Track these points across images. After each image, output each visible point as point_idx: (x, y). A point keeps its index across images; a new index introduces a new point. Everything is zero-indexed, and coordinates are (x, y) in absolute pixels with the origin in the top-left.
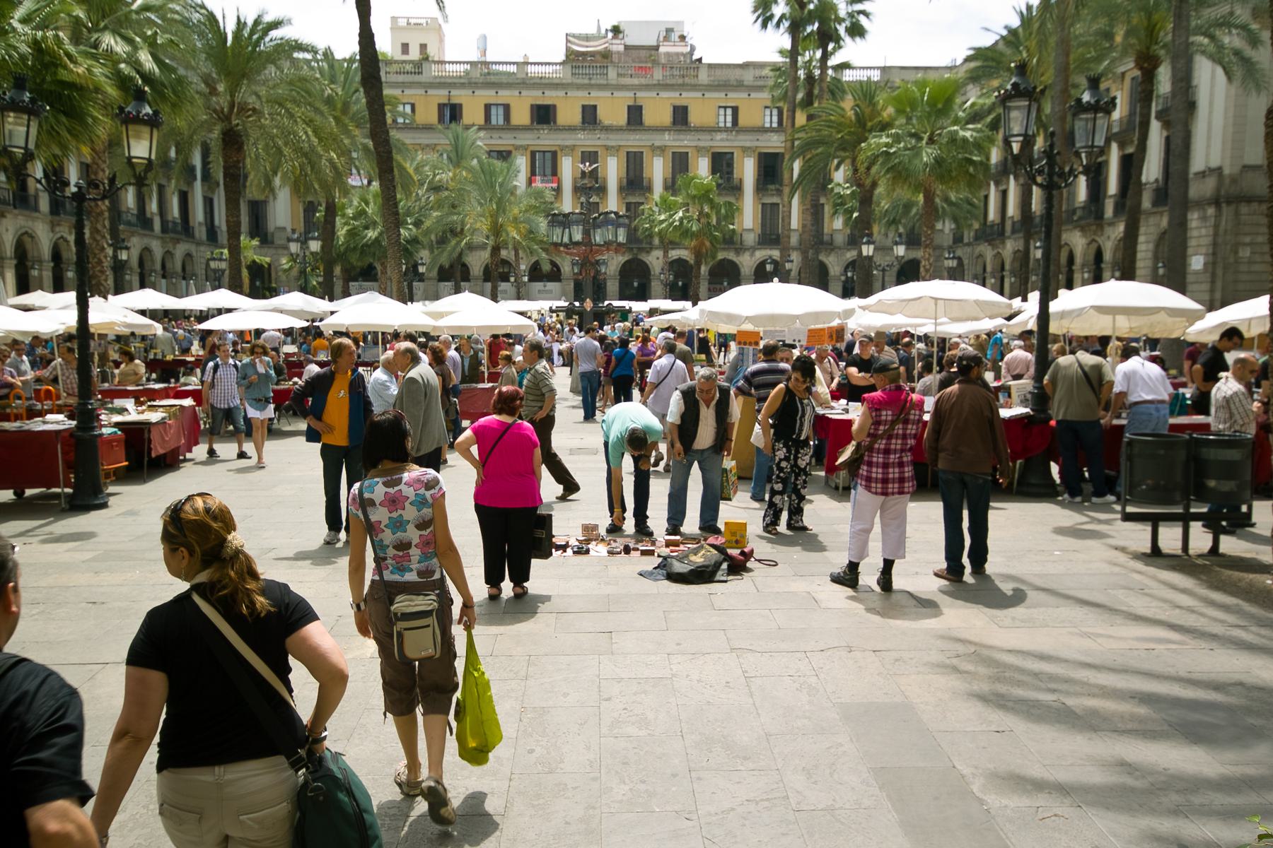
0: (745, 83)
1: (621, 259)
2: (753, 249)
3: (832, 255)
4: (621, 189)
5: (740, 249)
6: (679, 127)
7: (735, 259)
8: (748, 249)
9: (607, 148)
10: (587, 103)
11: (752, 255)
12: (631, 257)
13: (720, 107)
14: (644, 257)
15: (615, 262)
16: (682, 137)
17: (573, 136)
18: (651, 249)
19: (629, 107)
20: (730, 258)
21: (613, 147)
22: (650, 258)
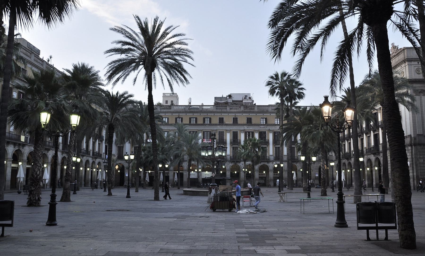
0: (269, 111)
3: (298, 163)
4: (231, 143)
5: (268, 161)
6: (249, 124)
7: (267, 165)
8: (271, 161)
9: (227, 130)
10: (221, 117)
13: (261, 118)
15: (229, 165)
16: (250, 127)
17: (216, 127)
19: (233, 118)
21: (228, 130)
22: (240, 164)
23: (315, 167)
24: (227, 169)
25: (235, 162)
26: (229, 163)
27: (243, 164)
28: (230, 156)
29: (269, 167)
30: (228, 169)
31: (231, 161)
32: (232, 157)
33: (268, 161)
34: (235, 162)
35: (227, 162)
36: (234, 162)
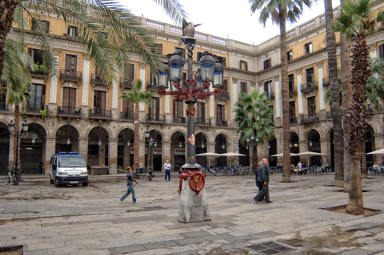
0: (166, 33)
1: (90, 127)
2: (170, 125)
3: (210, 131)
4: (91, 82)
5: (163, 124)
7: (160, 130)
8: (168, 125)
11: (169, 129)
12: (97, 126)
14: (105, 126)
15: (86, 129)
17: (61, 44)
18: (111, 120)
20: (158, 129)
22: (109, 127)
23: (234, 139)
24: (81, 136)
25: (100, 122)
26: (85, 123)
27: (114, 128)
28: (88, 109)
29: (163, 135)
30: (83, 136)
31: (90, 119)
32: (93, 111)
33: (163, 124)
34: (100, 122)
35: (82, 121)
36: (97, 120)
